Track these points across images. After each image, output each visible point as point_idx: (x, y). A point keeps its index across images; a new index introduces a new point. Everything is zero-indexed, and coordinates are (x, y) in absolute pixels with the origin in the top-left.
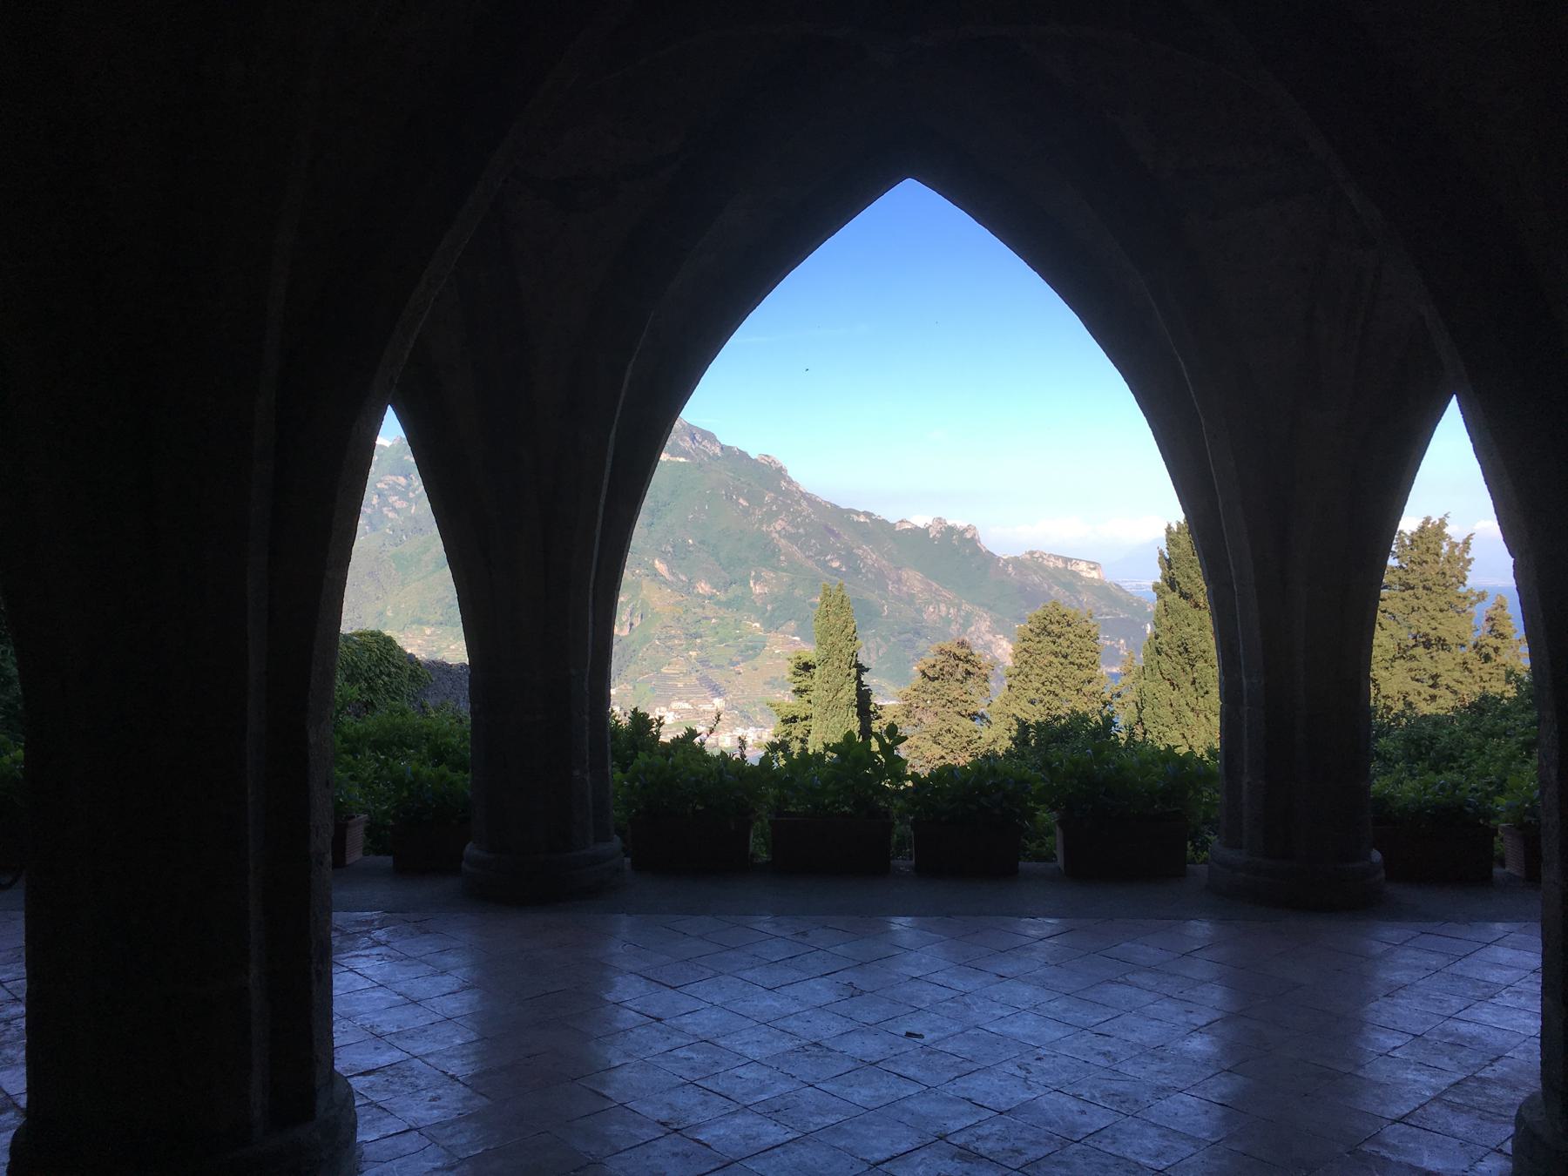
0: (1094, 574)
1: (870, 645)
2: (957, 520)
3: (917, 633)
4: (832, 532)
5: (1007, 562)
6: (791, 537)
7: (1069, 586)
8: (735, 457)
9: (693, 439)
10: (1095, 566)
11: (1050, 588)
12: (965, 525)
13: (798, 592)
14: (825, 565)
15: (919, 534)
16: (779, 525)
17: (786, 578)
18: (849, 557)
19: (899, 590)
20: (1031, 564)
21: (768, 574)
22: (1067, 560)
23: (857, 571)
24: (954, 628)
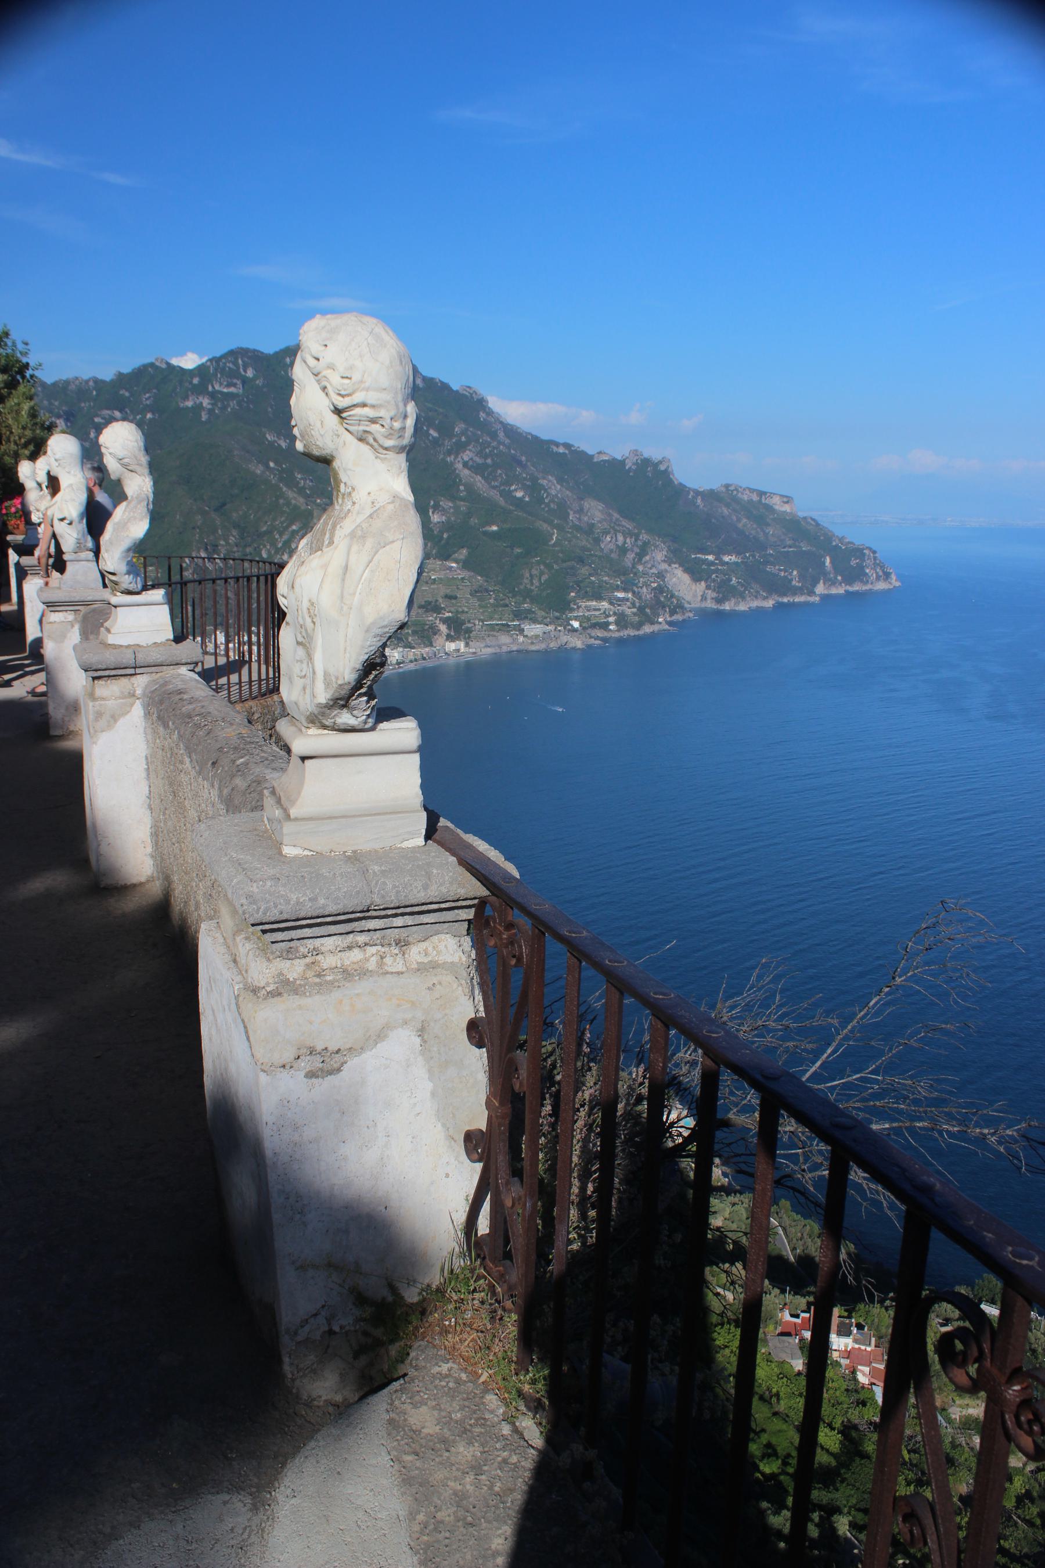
0: (787, 508)
1: (534, 572)
2: (652, 452)
3: (581, 561)
4: (519, 463)
5: (697, 493)
6: (477, 469)
10: (788, 500)
11: (739, 520)
12: (660, 458)
13: (474, 521)
14: (508, 495)
16: (467, 456)
17: (463, 506)
18: (534, 488)
19: (579, 519)
20: (726, 496)
22: (761, 494)
23: (540, 500)
24: (631, 556)
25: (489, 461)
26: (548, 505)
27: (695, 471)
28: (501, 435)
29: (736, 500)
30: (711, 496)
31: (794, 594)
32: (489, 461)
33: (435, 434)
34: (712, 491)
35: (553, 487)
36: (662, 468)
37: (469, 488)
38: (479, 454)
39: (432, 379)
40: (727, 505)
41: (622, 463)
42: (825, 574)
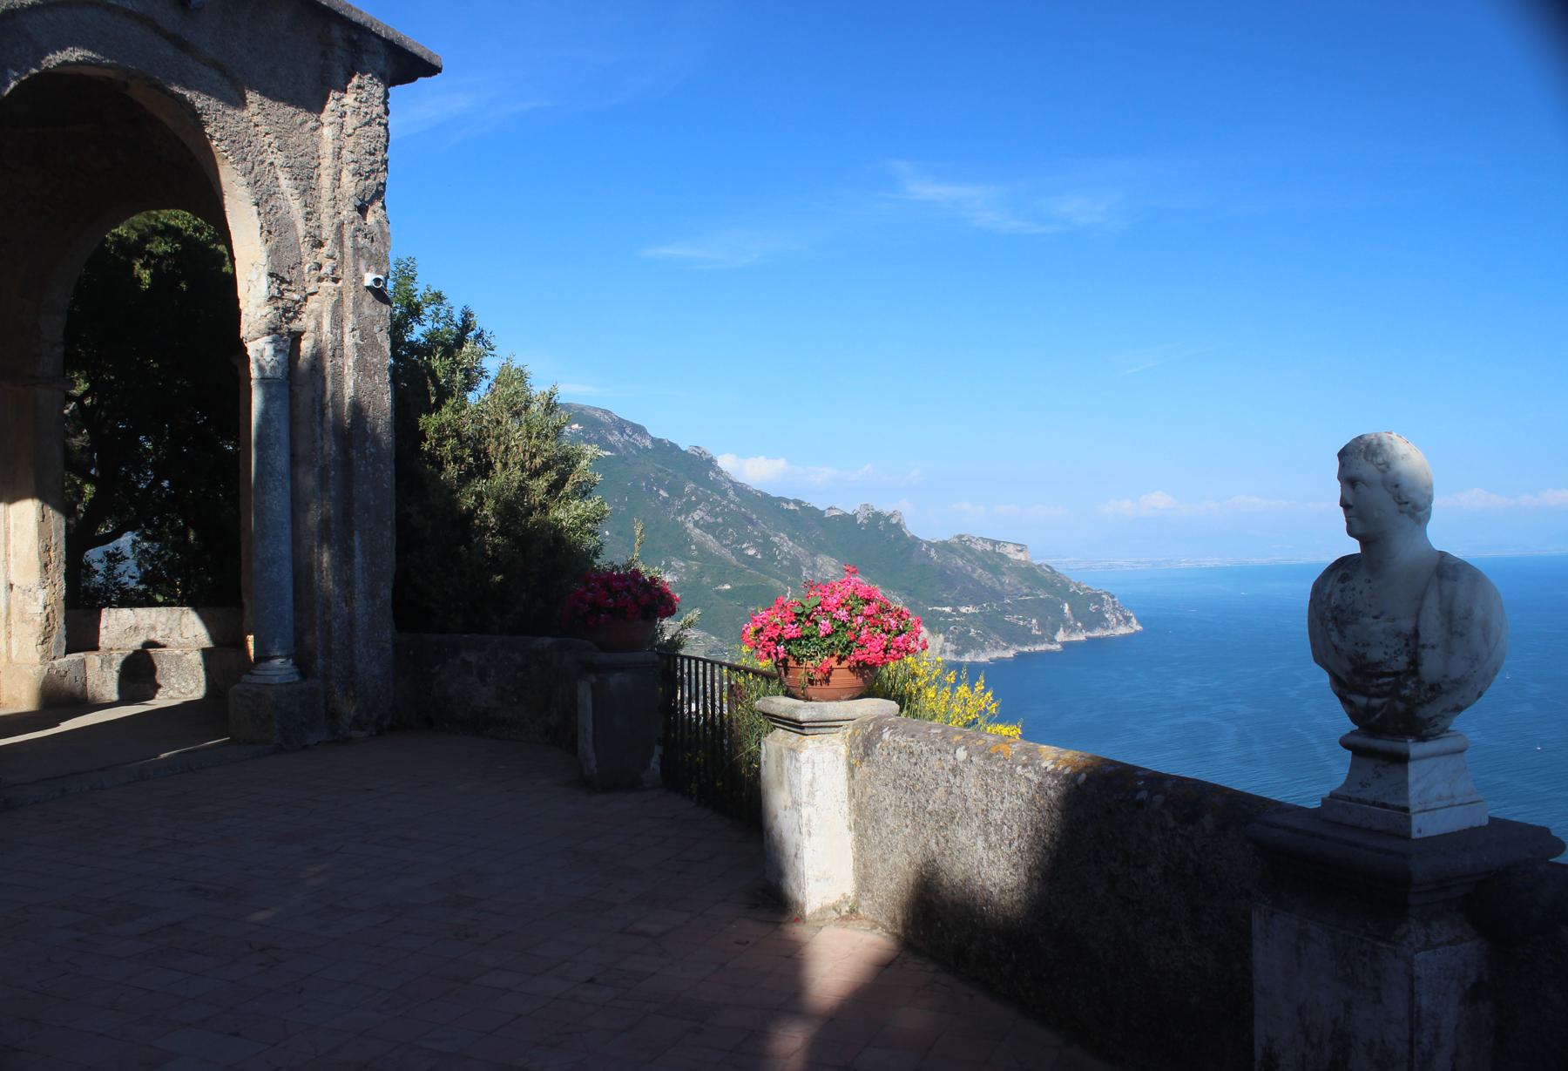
0: (1021, 556)
4: (750, 521)
7: (995, 570)
8: (665, 450)
9: (622, 432)
10: (1021, 548)
11: (974, 571)
13: (706, 580)
14: (740, 553)
15: (848, 520)
16: (697, 515)
18: (766, 545)
20: (959, 547)
21: (678, 564)
22: (995, 543)
23: (773, 558)
25: (720, 520)
26: (780, 562)
27: (928, 522)
28: (731, 493)
29: (969, 550)
30: (944, 547)
31: (1035, 643)
32: (720, 520)
33: (665, 495)
34: (945, 543)
35: (785, 544)
36: (894, 521)
37: (701, 547)
38: (710, 513)
39: (661, 440)
40: (962, 557)
41: (854, 517)
42: (1064, 621)
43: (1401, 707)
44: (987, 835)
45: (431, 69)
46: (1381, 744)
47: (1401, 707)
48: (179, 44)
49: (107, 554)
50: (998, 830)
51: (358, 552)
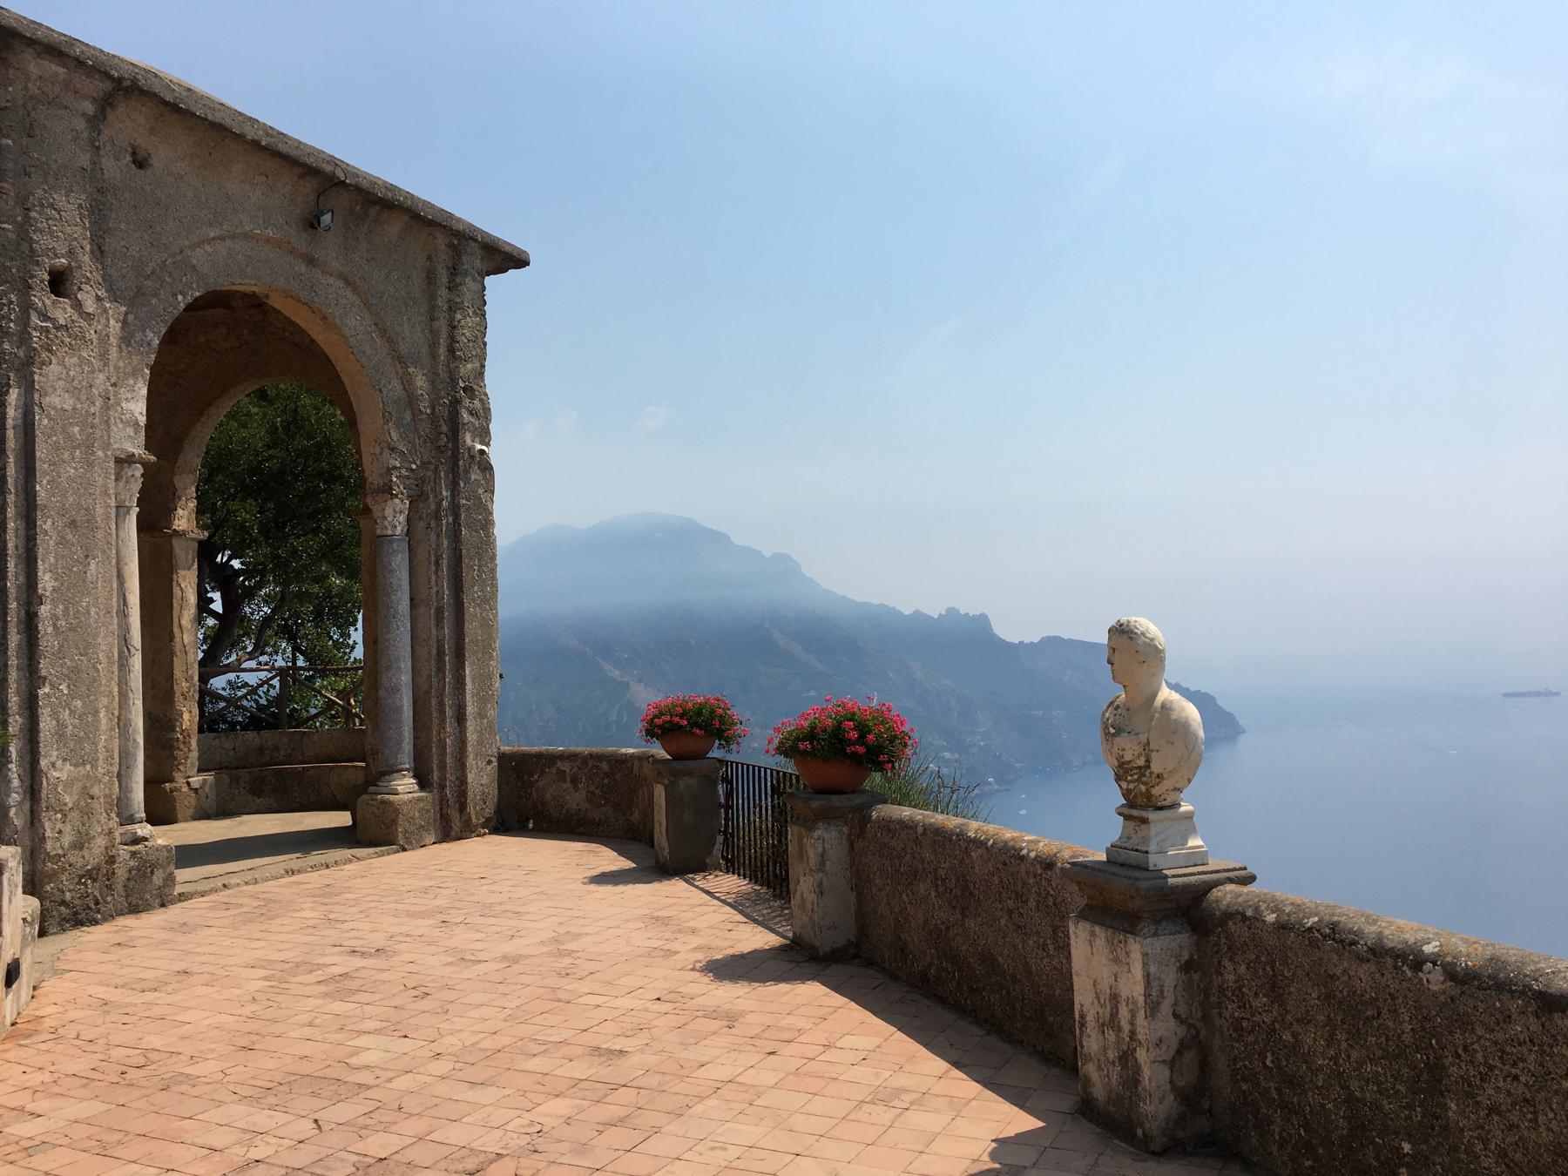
43: (1143, 788)
44: (937, 886)
45: (520, 261)
46: (1135, 813)
47: (1143, 788)
48: (311, 261)
49: (229, 682)
50: (943, 881)
51: (468, 680)
